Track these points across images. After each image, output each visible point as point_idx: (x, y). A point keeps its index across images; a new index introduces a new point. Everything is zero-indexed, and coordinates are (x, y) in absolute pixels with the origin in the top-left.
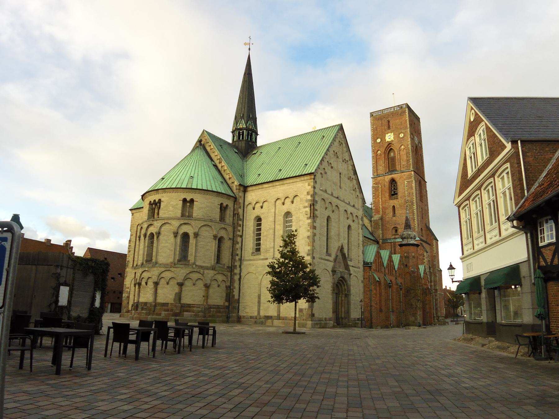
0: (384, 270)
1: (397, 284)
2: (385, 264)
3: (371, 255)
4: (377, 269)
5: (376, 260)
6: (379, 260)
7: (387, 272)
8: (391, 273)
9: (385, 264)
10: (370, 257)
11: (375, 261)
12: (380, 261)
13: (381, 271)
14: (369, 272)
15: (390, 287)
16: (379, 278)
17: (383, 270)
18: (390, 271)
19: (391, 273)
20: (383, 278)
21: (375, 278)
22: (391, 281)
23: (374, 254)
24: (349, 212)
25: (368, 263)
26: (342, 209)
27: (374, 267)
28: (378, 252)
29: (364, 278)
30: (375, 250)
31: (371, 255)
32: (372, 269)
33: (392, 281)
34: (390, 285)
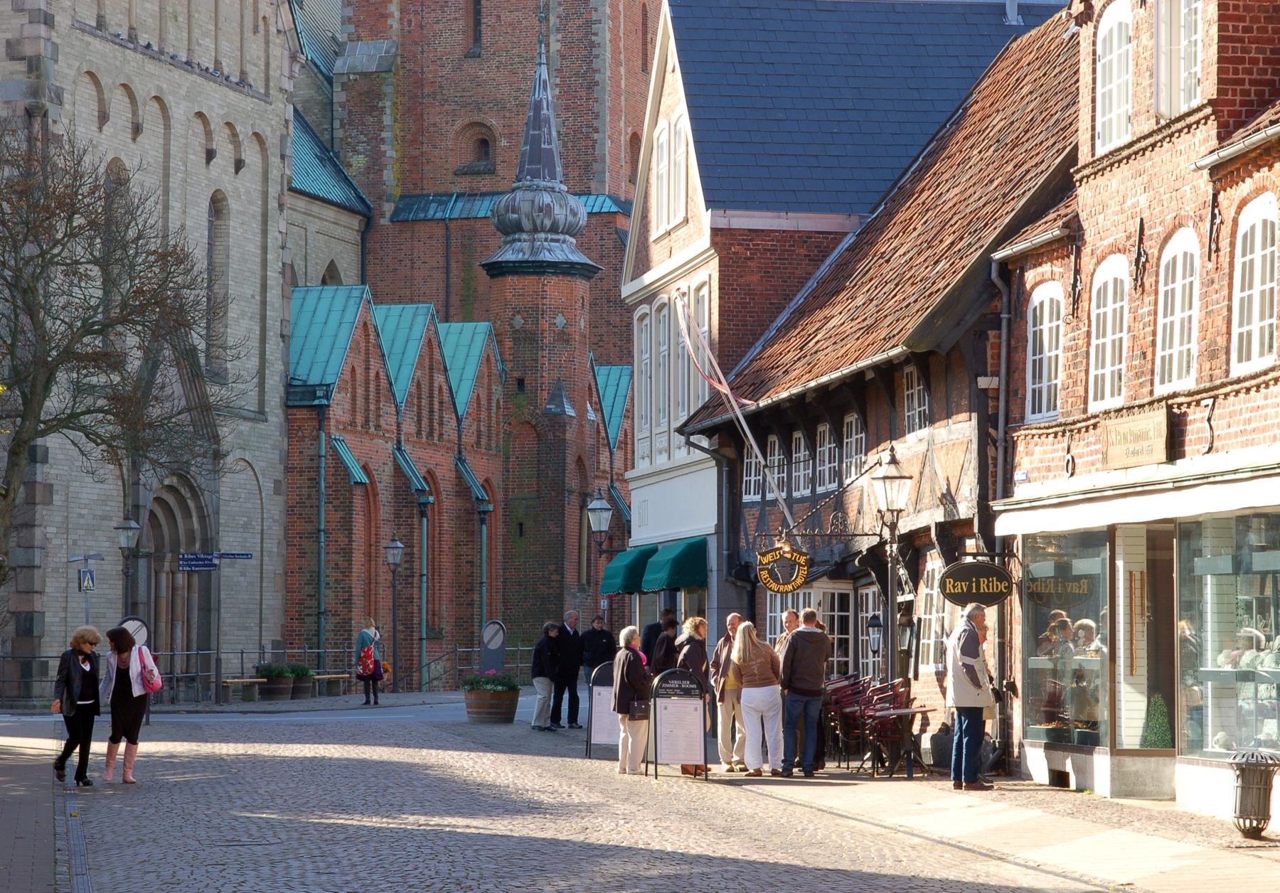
0: (392, 420)
1: (462, 489)
2: (402, 388)
3: (327, 342)
4: (360, 419)
5: (353, 369)
6: (367, 369)
7: (409, 427)
8: (431, 434)
9: (402, 388)
10: (322, 357)
11: (347, 377)
12: (372, 374)
13: (378, 427)
14: (318, 438)
15: (423, 510)
16: (365, 468)
17: (388, 421)
18: (425, 422)
19: (431, 434)
20: (390, 464)
21: (341, 468)
22: (430, 476)
23: (343, 340)
24: (216, 124)
25: (310, 391)
26: (180, 112)
27: (339, 409)
28: (365, 324)
29: (288, 470)
30: (353, 314)
31: (327, 342)
32: (333, 422)
33: (439, 473)
34: (422, 500)
